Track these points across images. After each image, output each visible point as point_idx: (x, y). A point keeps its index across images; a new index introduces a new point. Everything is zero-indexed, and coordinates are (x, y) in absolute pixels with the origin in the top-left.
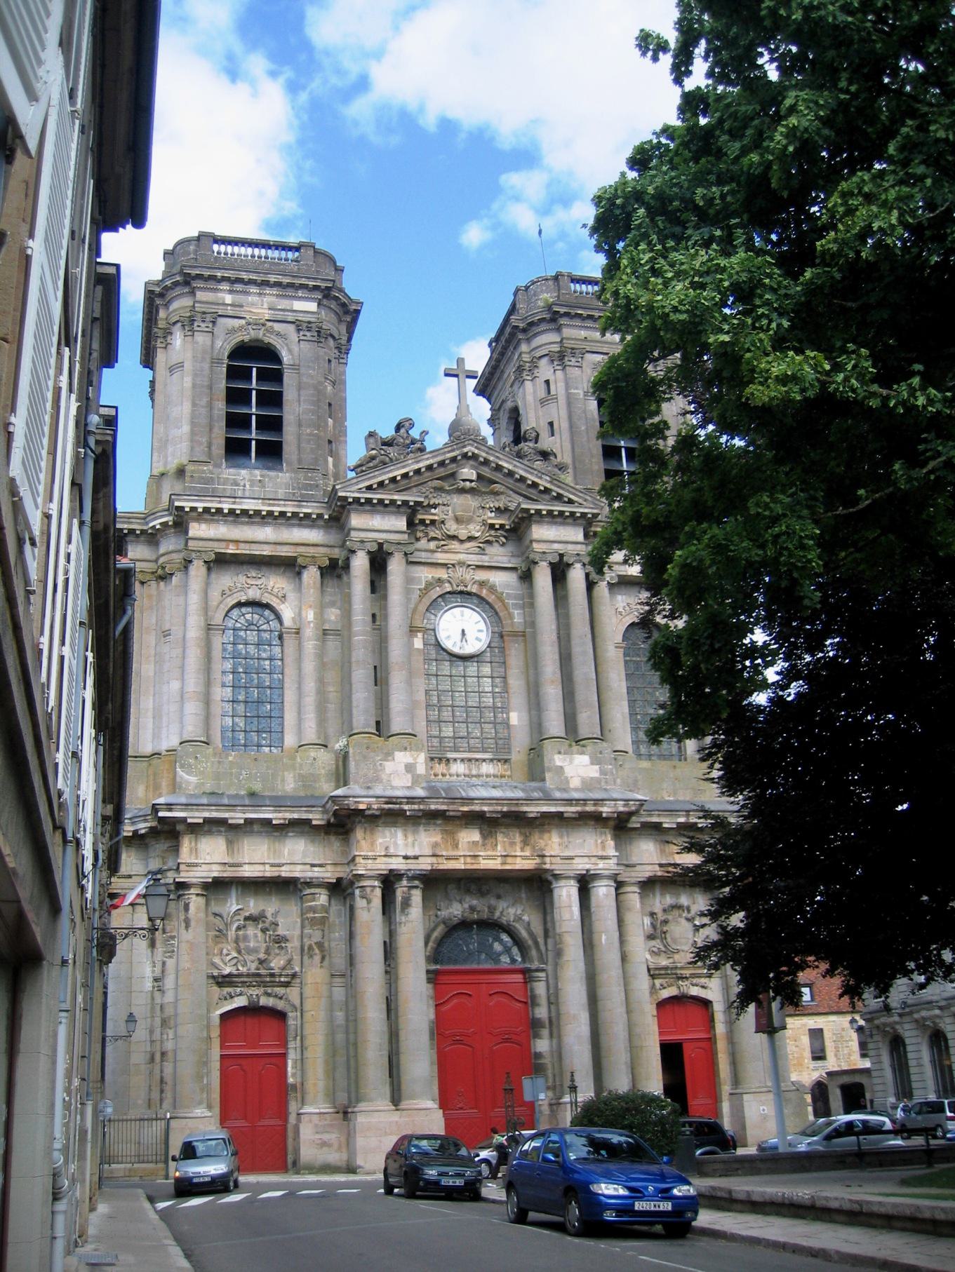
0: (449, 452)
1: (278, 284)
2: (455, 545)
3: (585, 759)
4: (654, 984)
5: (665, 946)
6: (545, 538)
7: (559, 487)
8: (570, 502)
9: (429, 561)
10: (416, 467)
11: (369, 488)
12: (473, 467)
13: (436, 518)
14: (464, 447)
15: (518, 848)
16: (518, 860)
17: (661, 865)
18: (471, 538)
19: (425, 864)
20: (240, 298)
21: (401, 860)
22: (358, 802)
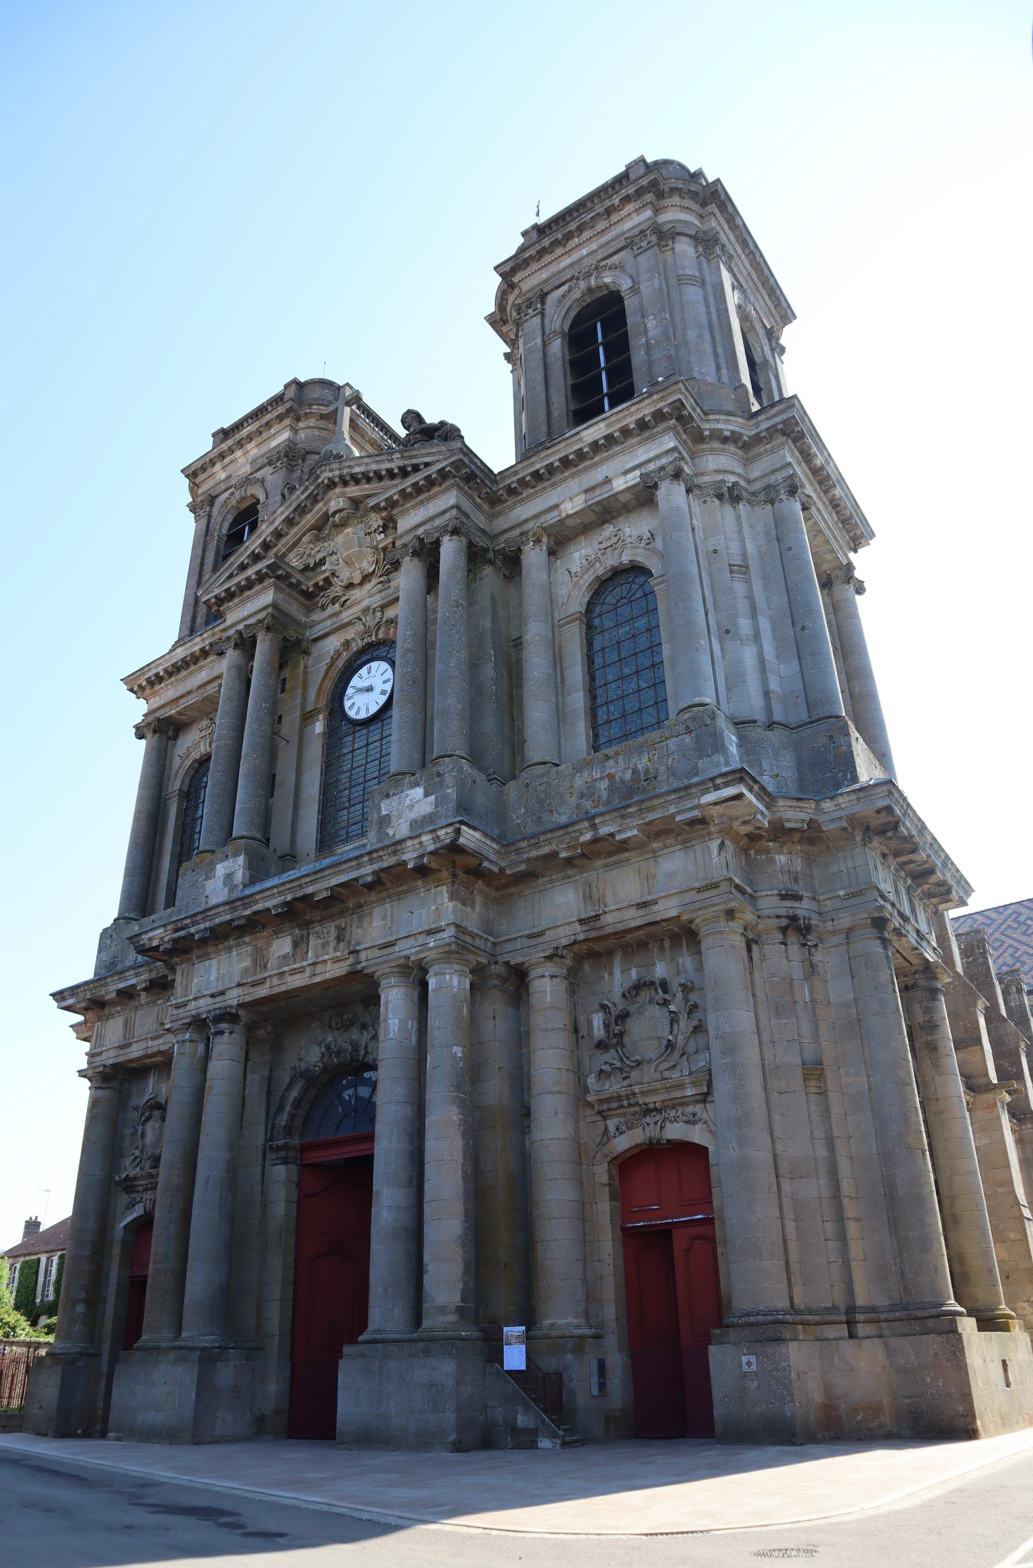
0: (303, 493)
1: (250, 438)
2: (356, 594)
3: (419, 792)
5: (622, 1060)
7: (412, 457)
8: (427, 465)
9: (334, 626)
11: (231, 576)
12: (343, 494)
13: (327, 574)
14: (318, 477)
15: (331, 949)
16: (329, 966)
17: (581, 921)
18: (366, 578)
19: (234, 998)
20: (230, 470)
21: (209, 1000)
22: (150, 939)
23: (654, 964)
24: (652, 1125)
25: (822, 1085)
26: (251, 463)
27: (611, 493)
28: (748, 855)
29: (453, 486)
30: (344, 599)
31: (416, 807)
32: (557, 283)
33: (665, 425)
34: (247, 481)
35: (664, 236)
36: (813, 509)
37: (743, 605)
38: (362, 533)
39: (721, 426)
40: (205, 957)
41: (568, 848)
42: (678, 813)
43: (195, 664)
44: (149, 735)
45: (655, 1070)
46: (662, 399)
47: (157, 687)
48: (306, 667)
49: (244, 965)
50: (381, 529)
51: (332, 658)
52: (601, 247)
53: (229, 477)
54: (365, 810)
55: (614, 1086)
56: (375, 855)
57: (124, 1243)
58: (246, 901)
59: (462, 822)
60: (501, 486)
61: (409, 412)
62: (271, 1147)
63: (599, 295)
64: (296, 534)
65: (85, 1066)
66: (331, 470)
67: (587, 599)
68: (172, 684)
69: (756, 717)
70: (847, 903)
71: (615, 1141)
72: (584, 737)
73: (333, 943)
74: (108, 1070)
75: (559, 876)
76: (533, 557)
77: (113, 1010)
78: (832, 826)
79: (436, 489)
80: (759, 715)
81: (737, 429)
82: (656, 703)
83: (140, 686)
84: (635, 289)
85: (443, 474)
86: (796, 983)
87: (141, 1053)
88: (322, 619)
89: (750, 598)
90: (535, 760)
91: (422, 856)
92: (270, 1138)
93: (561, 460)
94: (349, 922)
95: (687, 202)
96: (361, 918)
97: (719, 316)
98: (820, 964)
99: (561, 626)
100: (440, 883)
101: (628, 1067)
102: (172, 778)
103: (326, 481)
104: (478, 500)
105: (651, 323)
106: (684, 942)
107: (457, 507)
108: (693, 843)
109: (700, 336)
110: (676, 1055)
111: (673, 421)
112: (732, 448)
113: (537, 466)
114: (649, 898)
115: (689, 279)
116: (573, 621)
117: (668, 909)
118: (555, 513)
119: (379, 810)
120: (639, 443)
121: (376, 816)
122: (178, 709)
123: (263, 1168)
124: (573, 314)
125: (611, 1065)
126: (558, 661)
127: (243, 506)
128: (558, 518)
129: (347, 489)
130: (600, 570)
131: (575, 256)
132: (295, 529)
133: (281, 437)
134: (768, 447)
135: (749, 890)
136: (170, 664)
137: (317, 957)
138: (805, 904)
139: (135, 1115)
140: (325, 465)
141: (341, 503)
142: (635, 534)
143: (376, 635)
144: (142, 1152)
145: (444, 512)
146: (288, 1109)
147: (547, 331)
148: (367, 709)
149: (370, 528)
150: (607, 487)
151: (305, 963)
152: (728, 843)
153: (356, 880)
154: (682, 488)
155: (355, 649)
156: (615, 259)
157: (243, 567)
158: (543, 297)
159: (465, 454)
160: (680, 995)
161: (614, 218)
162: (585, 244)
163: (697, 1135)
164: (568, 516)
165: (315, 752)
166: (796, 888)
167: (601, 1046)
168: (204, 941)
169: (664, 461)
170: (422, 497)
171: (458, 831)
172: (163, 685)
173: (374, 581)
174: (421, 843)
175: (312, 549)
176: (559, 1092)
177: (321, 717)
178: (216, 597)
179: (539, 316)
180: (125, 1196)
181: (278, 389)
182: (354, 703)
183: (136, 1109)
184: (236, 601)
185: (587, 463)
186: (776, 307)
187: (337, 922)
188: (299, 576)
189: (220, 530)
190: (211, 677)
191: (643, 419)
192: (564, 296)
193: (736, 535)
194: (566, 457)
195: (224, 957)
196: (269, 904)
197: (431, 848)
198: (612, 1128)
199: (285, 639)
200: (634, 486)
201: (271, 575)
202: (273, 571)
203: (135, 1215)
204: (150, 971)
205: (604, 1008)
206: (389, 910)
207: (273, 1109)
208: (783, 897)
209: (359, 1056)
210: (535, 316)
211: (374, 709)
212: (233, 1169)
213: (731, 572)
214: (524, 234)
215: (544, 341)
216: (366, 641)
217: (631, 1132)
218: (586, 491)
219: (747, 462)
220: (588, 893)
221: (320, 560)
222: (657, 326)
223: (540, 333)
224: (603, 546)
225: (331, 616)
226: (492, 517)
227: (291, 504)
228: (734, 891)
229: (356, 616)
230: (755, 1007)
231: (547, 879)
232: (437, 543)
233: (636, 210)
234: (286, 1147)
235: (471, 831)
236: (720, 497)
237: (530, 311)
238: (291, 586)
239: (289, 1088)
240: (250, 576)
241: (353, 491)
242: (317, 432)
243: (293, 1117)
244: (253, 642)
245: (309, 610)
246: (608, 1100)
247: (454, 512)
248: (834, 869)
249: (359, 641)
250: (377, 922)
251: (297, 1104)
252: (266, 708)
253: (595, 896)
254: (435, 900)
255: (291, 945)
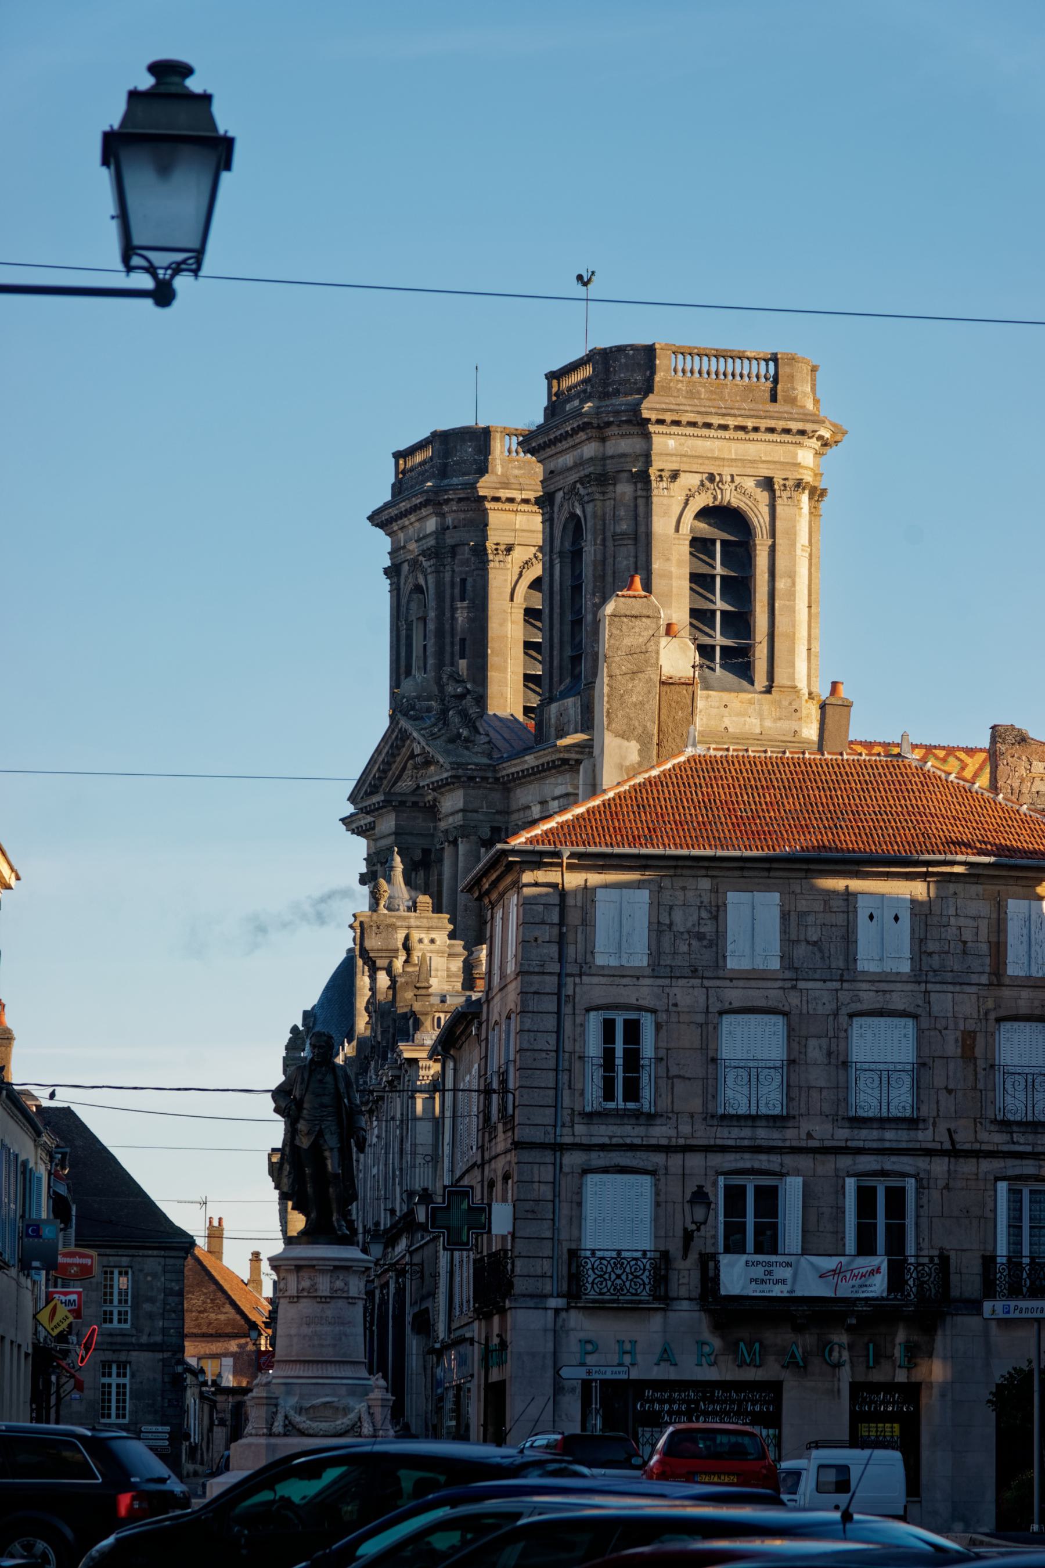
64: (400, 762)
95: (626, 428)
132: (398, 759)
181: (426, 434)
242: (462, 516)
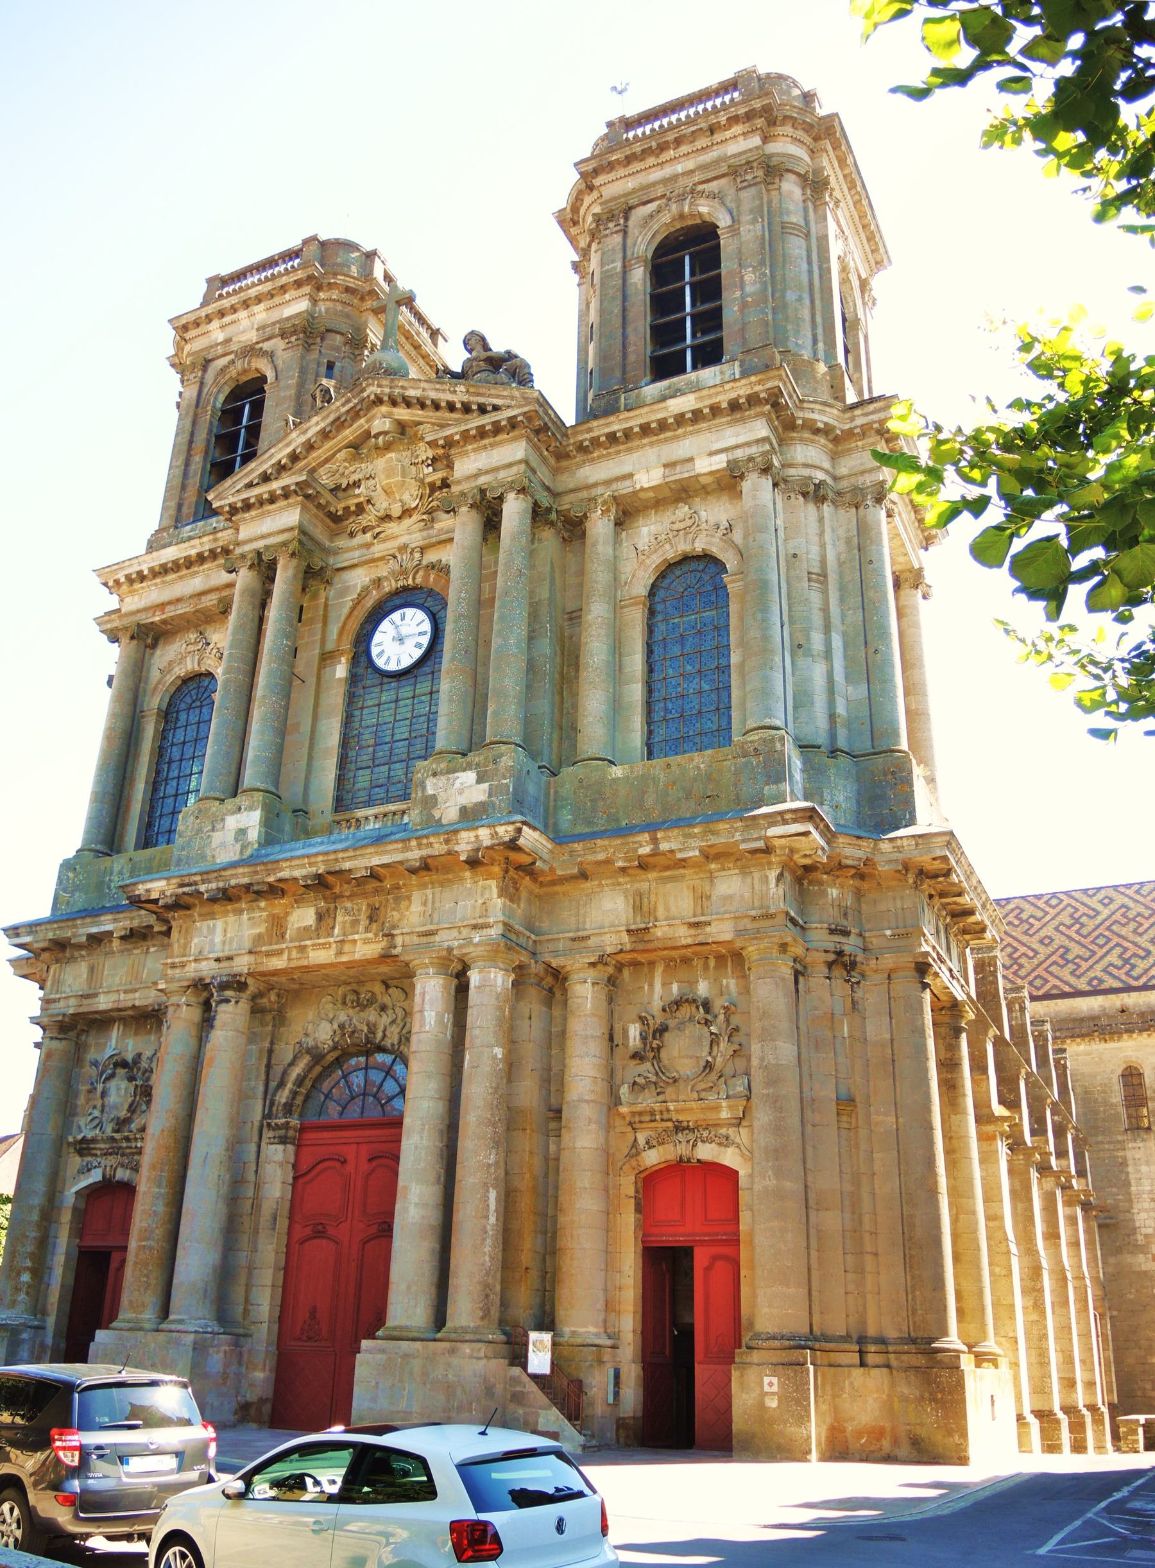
0: (343, 405)
1: (259, 299)
2: (392, 528)
3: (470, 776)
4: (635, 1140)
5: (657, 1074)
6: (468, 473)
7: (479, 395)
8: (496, 408)
9: (363, 559)
10: (303, 439)
13: (362, 499)
14: (363, 390)
15: (361, 928)
18: (407, 513)
19: (242, 964)
20: (230, 331)
21: (213, 964)
22: (148, 891)
23: (697, 981)
24: (684, 1144)
25: (854, 1120)
26: (258, 330)
27: (693, 474)
28: (801, 884)
29: (522, 436)
30: (377, 530)
31: (467, 792)
32: (645, 198)
33: (758, 409)
34: (250, 351)
35: (773, 170)
36: (897, 518)
37: (817, 618)
38: (407, 462)
39: (815, 416)
40: (212, 916)
41: (626, 860)
42: (743, 841)
43: (188, 568)
44: (125, 640)
45: (692, 1090)
46: (759, 382)
47: (137, 586)
48: (327, 599)
49: (258, 931)
50: (430, 462)
51: (359, 595)
52: (703, 167)
53: (228, 341)
54: (392, 773)
55: (648, 1101)
56: (425, 841)
57: (75, 1209)
58: (270, 866)
59: (524, 823)
60: (572, 441)
61: (472, 333)
62: (269, 1125)
63: (690, 222)
64: (331, 448)
65: (37, 1013)
66: (379, 386)
67: (651, 581)
68: (156, 585)
69: (820, 741)
70: (893, 944)
71: (643, 1154)
72: (639, 733)
73: (364, 922)
74: (67, 1020)
75: (609, 881)
76: (600, 526)
77: (76, 954)
78: (887, 868)
79: (502, 437)
80: (822, 739)
81: (831, 421)
82: (718, 709)
83: (117, 582)
84: (734, 229)
85: (513, 424)
86: (837, 1016)
87: (110, 1006)
88: (349, 549)
89: (825, 610)
90: (590, 754)
91: (478, 850)
92: (267, 1116)
93: (642, 426)
94: (384, 903)
96: (397, 900)
97: (821, 277)
98: (860, 1002)
99: (622, 607)
100: (491, 876)
101: (663, 1082)
102: (149, 692)
103: (372, 397)
104: (546, 453)
105: (749, 277)
106: (729, 964)
107: (527, 462)
108: (752, 869)
109: (800, 299)
110: (713, 1076)
111: (768, 407)
112: (823, 441)
113: (615, 428)
114: (702, 919)
115: (794, 229)
116: (636, 604)
117: (721, 931)
118: (628, 483)
119: (424, 788)
120: (728, 423)
121: (420, 794)
122: (163, 617)
123: (259, 1146)
124: (659, 238)
125: (646, 1078)
126: (617, 648)
127: (245, 378)
128: (631, 490)
129: (395, 410)
130: (671, 553)
131: (668, 171)
133: (297, 306)
134: (860, 443)
135: (801, 922)
136: (158, 563)
137: (344, 935)
138: (853, 939)
139: (94, 1072)
140: (373, 378)
141: (388, 425)
142: (712, 521)
143: (414, 578)
144: (102, 1111)
145: (510, 465)
146: (289, 1085)
147: (629, 253)
148: (399, 661)
149: (417, 457)
150: (689, 465)
151: (331, 940)
152: (786, 874)
153: (401, 863)
154: (770, 483)
155: (387, 589)
156: (713, 186)
157: (266, 478)
158: (627, 211)
159: (541, 405)
160: (721, 1017)
161: (718, 137)
162: (681, 160)
163: (729, 1158)
164: (642, 489)
165: (335, 698)
166: (845, 923)
167: (636, 1056)
168: (213, 900)
169: (754, 450)
170: (486, 442)
171: (519, 831)
172: (144, 584)
173: (415, 517)
174: (477, 837)
175: (346, 468)
176: (593, 1101)
177: (343, 660)
178: (230, 505)
179: (621, 234)
180: (78, 1159)
182: (383, 651)
183: (95, 1064)
184: (253, 513)
185: (669, 434)
186: (872, 251)
187: (371, 900)
188: (329, 497)
189: (214, 402)
190: (207, 587)
191: (736, 400)
192: (651, 216)
193: (817, 538)
194: (648, 424)
195: (231, 919)
196: (297, 873)
197: (487, 842)
198: (641, 1139)
199: (309, 566)
200: (718, 471)
201: (300, 493)
202: (301, 489)
203: (90, 1181)
204: (132, 919)
205: (642, 1020)
206: (430, 897)
207: (273, 1085)
208: (832, 932)
209: (375, 1038)
210: (616, 232)
211: (406, 662)
212: (234, 1146)
213: (809, 580)
214: (610, 125)
215: (624, 266)
216: (400, 583)
217: (661, 1148)
218: (665, 466)
219: (834, 456)
220: (638, 903)
221: (355, 483)
222: (755, 282)
223: (620, 255)
224: (676, 526)
225: (360, 546)
226: (556, 472)
227: (328, 416)
228: (789, 924)
229: (391, 552)
230: (798, 1040)
231: (596, 883)
232: (501, 499)
233: (744, 134)
234: (286, 1126)
235: (530, 831)
236: (805, 495)
237: (611, 225)
238: (319, 506)
239: (292, 1064)
240: (275, 491)
241: (402, 413)
242: (339, 307)
243: (294, 1094)
244: (272, 566)
245: (334, 535)
246: (640, 1113)
247: (523, 467)
248: (882, 906)
249: (393, 582)
250: (416, 907)
251: (300, 1082)
252: (287, 646)
253: (645, 909)
254: (482, 895)
255: (314, 917)
